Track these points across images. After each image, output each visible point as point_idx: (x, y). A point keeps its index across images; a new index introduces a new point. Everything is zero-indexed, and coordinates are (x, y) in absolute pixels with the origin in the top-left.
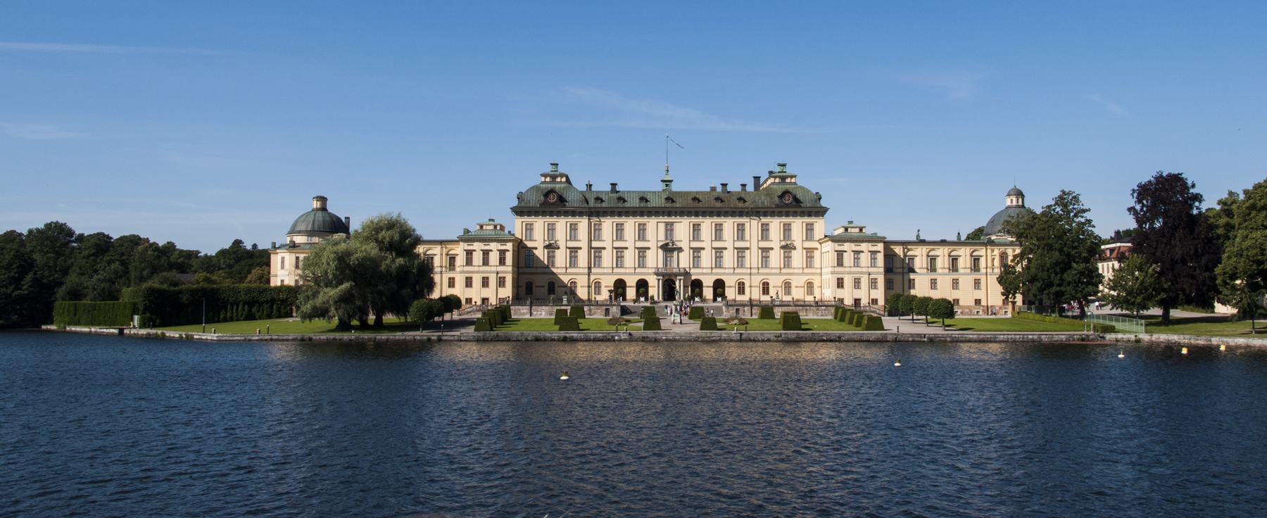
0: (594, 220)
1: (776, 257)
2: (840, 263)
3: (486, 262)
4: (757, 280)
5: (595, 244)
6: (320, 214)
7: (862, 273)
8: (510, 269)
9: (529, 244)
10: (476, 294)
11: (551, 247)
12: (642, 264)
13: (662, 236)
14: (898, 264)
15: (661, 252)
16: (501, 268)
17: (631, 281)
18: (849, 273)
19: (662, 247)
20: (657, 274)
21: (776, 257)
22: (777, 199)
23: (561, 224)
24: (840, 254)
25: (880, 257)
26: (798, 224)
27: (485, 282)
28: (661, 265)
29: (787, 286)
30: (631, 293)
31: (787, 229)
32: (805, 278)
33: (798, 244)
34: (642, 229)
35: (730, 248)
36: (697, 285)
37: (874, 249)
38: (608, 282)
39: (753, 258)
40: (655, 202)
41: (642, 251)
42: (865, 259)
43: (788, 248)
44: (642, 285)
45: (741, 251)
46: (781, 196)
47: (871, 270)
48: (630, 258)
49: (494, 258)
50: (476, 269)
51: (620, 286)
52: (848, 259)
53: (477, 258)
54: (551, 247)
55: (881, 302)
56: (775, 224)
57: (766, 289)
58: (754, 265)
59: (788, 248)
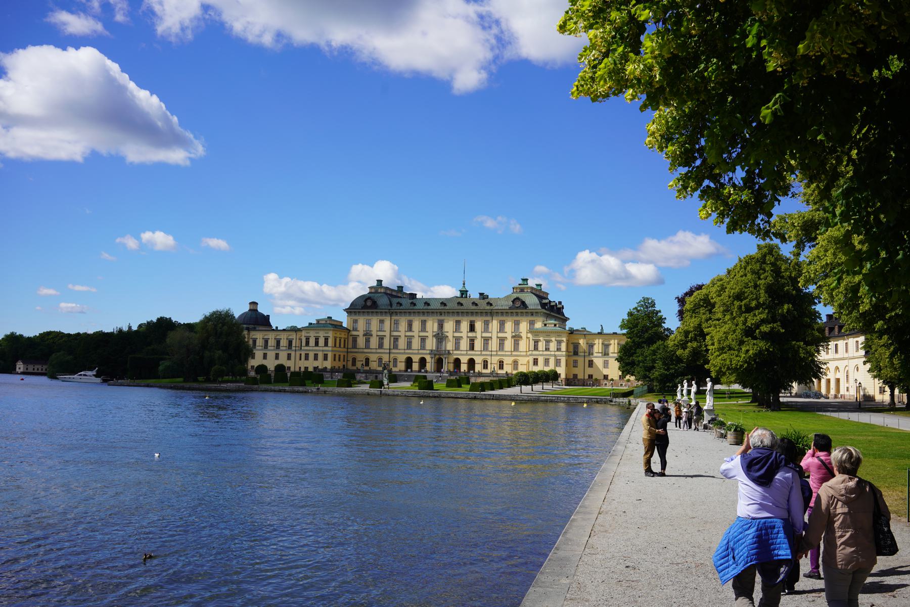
0: (394, 318)
1: (509, 345)
2: (536, 348)
3: (317, 344)
4: (495, 360)
5: (395, 334)
7: (551, 355)
9: (354, 333)
10: (311, 365)
12: (423, 347)
13: (436, 329)
14: (580, 350)
15: (435, 340)
17: (416, 359)
18: (541, 355)
21: (509, 345)
23: (375, 321)
24: (536, 342)
25: (563, 346)
29: (515, 364)
30: (415, 366)
32: (483, 357)
33: (524, 335)
34: (424, 323)
36: (457, 362)
38: (402, 358)
39: (494, 345)
40: (451, 306)
41: (423, 340)
42: (553, 346)
44: (423, 362)
46: (513, 302)
48: (416, 344)
49: (321, 342)
51: (409, 362)
52: (542, 345)
53: (312, 342)
57: (501, 366)
58: (494, 349)
59: (517, 338)
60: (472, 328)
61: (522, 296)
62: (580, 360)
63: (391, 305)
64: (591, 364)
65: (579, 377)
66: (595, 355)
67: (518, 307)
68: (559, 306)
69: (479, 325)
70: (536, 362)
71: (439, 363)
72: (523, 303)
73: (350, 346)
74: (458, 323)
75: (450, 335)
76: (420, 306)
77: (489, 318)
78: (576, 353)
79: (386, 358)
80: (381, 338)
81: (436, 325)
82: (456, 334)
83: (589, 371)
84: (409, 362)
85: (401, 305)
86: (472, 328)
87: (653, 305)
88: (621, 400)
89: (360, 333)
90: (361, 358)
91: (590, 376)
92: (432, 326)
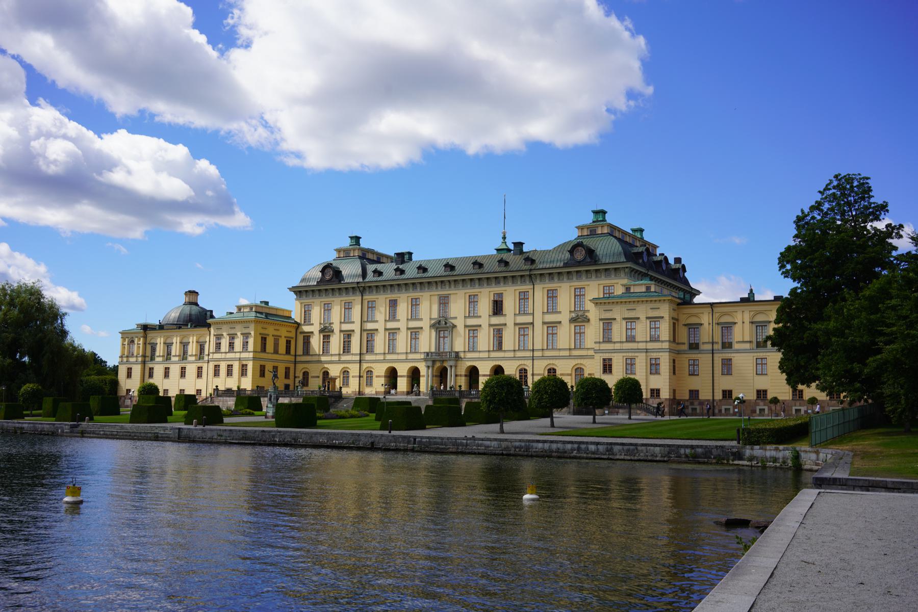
0: (368, 297)
6: (188, 308)
7: (638, 350)
8: (251, 355)
11: (326, 332)
13: (435, 315)
15: (434, 333)
16: (244, 355)
17: (403, 370)
19: (432, 326)
20: (425, 360)
22: (568, 255)
26: (593, 288)
27: (229, 373)
28: (433, 350)
30: (403, 384)
31: (579, 295)
35: (510, 324)
37: (655, 314)
38: (380, 370)
39: (539, 336)
42: (642, 330)
43: (579, 319)
44: (414, 375)
45: (523, 328)
47: (651, 346)
50: (223, 356)
51: (392, 375)
52: (618, 331)
54: (326, 332)
55: (665, 394)
56: (565, 292)
60: (497, 308)
61: (590, 243)
62: (704, 360)
63: (364, 274)
64: (727, 366)
65: (702, 396)
66: (736, 346)
67: (581, 259)
68: (678, 266)
69: (510, 304)
70: (607, 367)
71: (442, 375)
72: (591, 252)
73: (300, 351)
74: (473, 301)
75: (460, 323)
76: (411, 271)
77: (527, 287)
78: (694, 347)
79: (354, 370)
80: (347, 336)
81: (435, 307)
82: (471, 322)
83: (724, 383)
84: (392, 375)
85: (380, 274)
86: (497, 308)
87: (865, 190)
88: (770, 451)
89: (314, 328)
90: (315, 371)
91: (727, 394)
92: (429, 308)
